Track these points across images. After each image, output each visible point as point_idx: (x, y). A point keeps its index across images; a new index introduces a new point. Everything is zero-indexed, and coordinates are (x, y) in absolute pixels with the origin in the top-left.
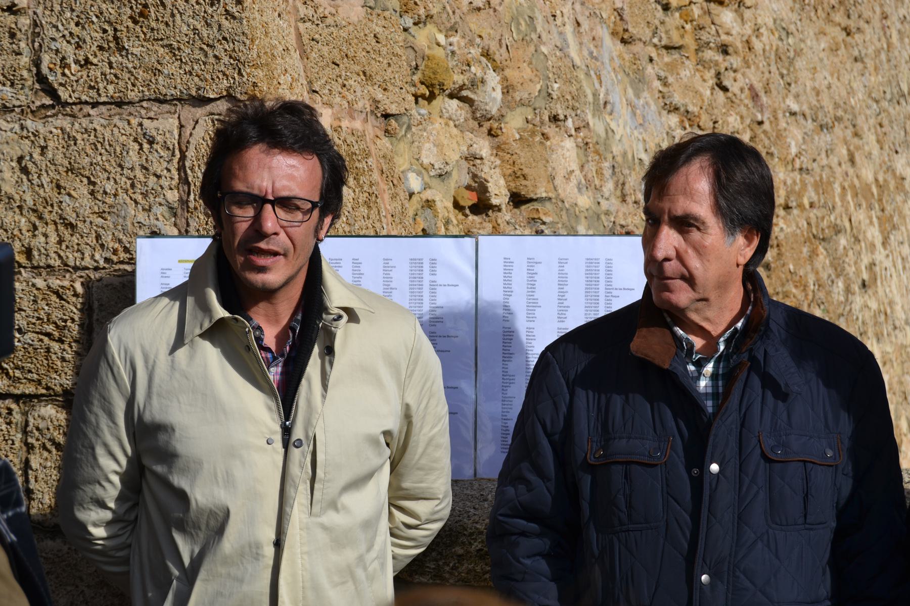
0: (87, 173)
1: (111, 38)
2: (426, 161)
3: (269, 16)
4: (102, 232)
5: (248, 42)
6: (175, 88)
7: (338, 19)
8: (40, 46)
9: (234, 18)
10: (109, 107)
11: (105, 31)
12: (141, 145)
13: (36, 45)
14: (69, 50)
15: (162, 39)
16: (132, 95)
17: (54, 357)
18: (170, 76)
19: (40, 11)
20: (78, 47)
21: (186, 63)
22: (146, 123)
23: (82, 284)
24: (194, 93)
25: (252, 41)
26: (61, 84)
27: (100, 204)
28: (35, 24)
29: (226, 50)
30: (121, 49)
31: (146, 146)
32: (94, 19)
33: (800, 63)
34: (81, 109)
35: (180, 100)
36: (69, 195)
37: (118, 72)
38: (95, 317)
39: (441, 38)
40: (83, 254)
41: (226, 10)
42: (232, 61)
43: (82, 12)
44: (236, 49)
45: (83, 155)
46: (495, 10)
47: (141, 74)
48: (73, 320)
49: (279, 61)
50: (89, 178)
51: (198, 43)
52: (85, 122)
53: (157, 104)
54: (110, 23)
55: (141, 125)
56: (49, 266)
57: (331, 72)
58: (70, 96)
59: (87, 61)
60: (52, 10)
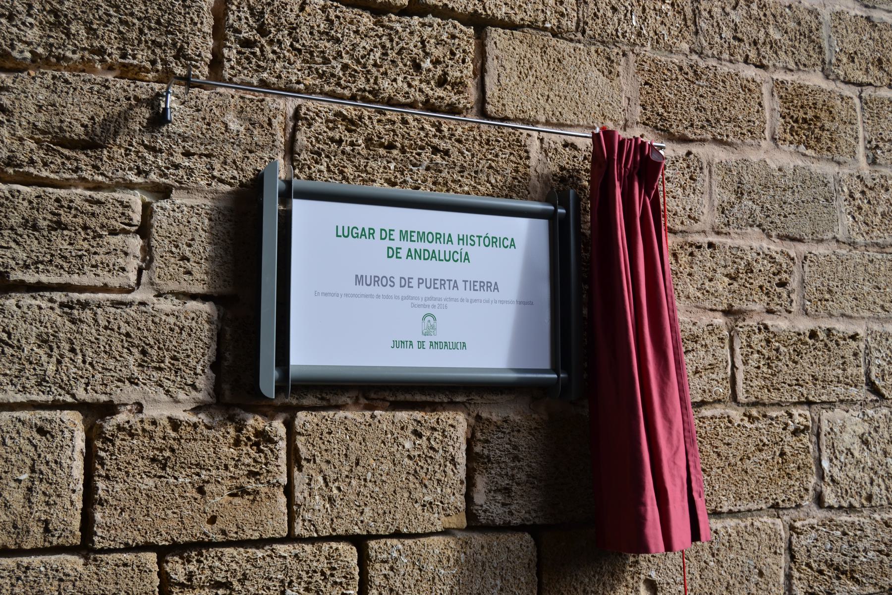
19: (869, 339)
56: (882, 505)
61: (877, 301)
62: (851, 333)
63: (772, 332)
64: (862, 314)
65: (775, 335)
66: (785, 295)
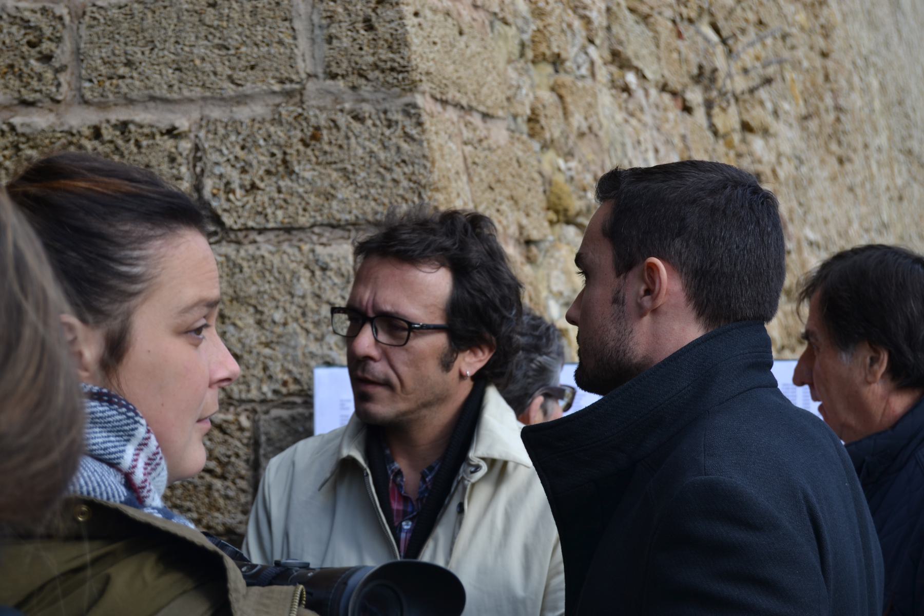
0: (253, 302)
1: (279, 162)
2: (555, 288)
3: (443, 137)
4: (270, 363)
5: (429, 165)
6: (350, 212)
7: (491, 141)
8: (203, 171)
9: (414, 140)
10: (277, 232)
11: (273, 155)
12: (313, 272)
13: (198, 169)
14: (234, 176)
15: (335, 163)
16: (303, 221)
17: (216, 495)
18: (344, 201)
19: (202, 134)
20: (244, 171)
21: (361, 187)
22: (319, 249)
23: (248, 418)
24: (370, 218)
25: (433, 163)
26: (225, 210)
27: (268, 334)
28: (197, 148)
29: (405, 174)
30: (291, 172)
31: (318, 273)
32: (262, 142)
33: (812, 193)
34: (246, 236)
35: (354, 224)
36: (234, 325)
37: (288, 197)
38: (262, 452)
39: (561, 163)
40: (249, 386)
41: (405, 133)
42: (412, 185)
43: (248, 136)
44: (417, 172)
45: (249, 282)
46: (596, 136)
47: (313, 199)
48: (237, 456)
49: (454, 185)
50: (255, 307)
51: (375, 167)
52: (251, 249)
53: (330, 229)
54: (279, 145)
55: (313, 251)
57: (489, 195)
58: (236, 222)
59: (254, 186)
60: (216, 134)
61: (219, 69)
62: (164, 126)
63: (23, 135)
64: (186, 93)
65: (28, 140)
66: (49, 75)
